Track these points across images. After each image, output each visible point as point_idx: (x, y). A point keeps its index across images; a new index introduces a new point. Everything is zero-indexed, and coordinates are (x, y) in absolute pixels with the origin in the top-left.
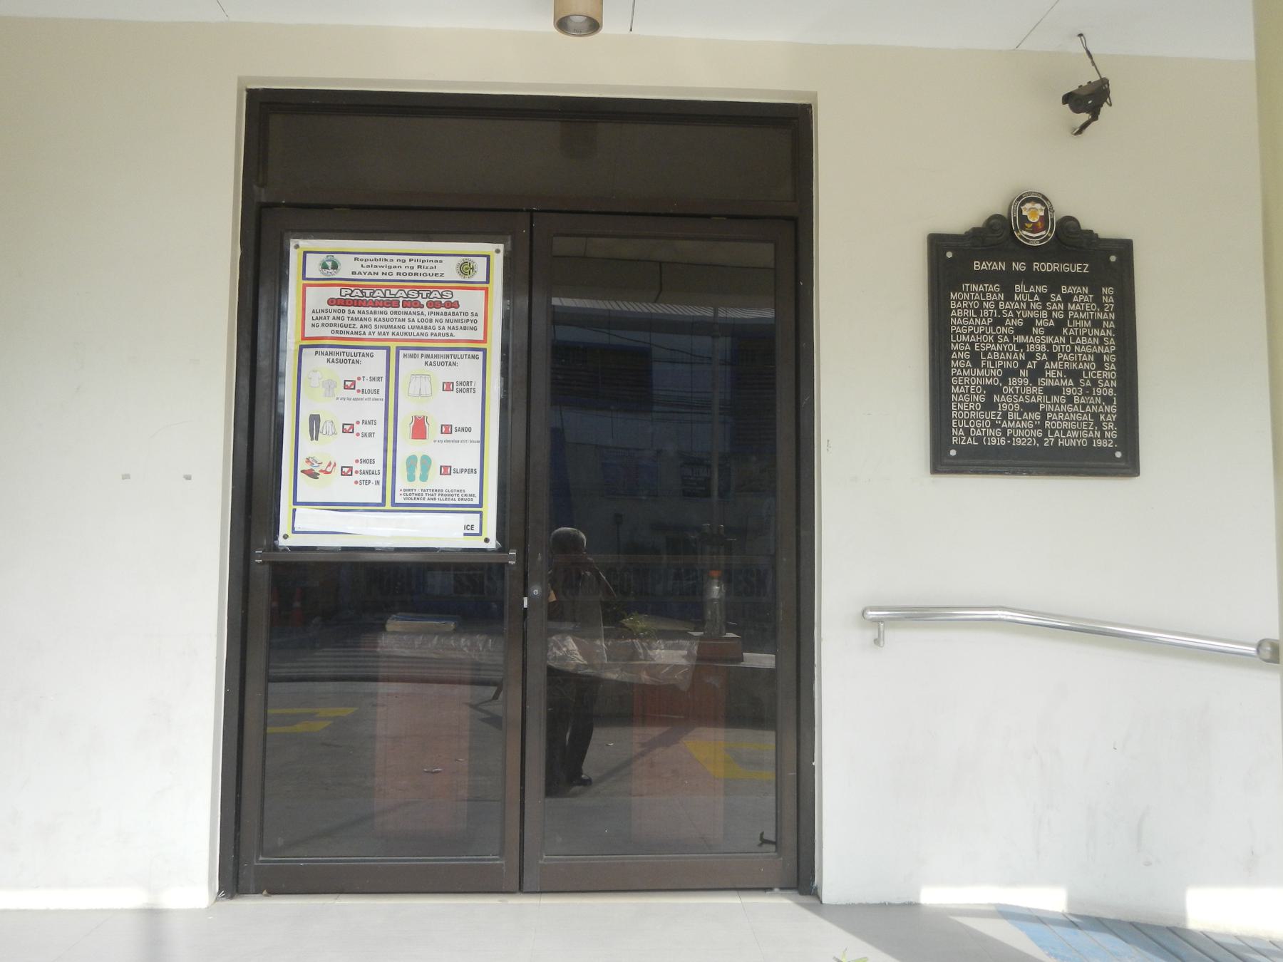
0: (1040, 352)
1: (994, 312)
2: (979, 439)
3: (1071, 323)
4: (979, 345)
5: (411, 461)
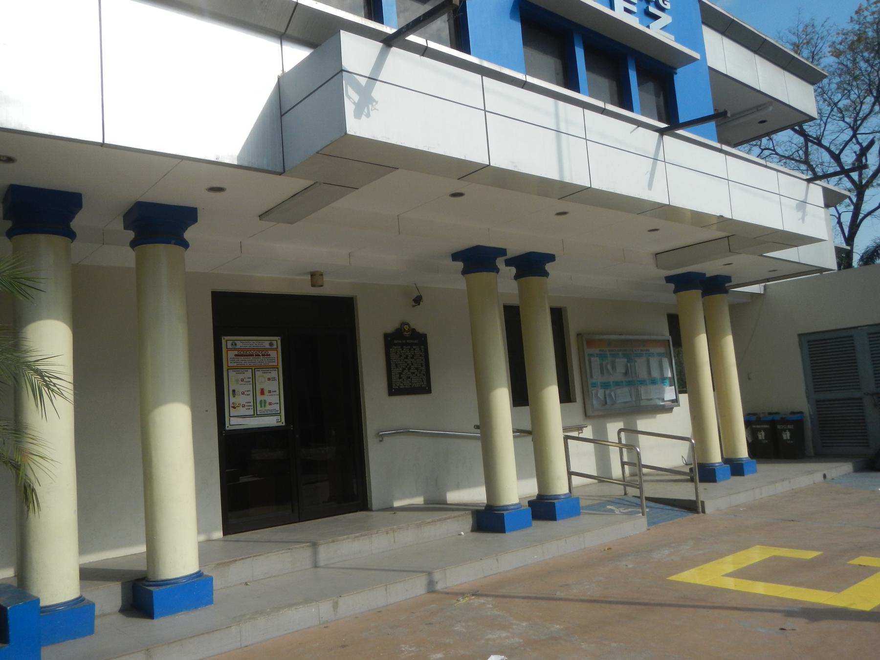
2: (398, 386)
5: (261, 402)
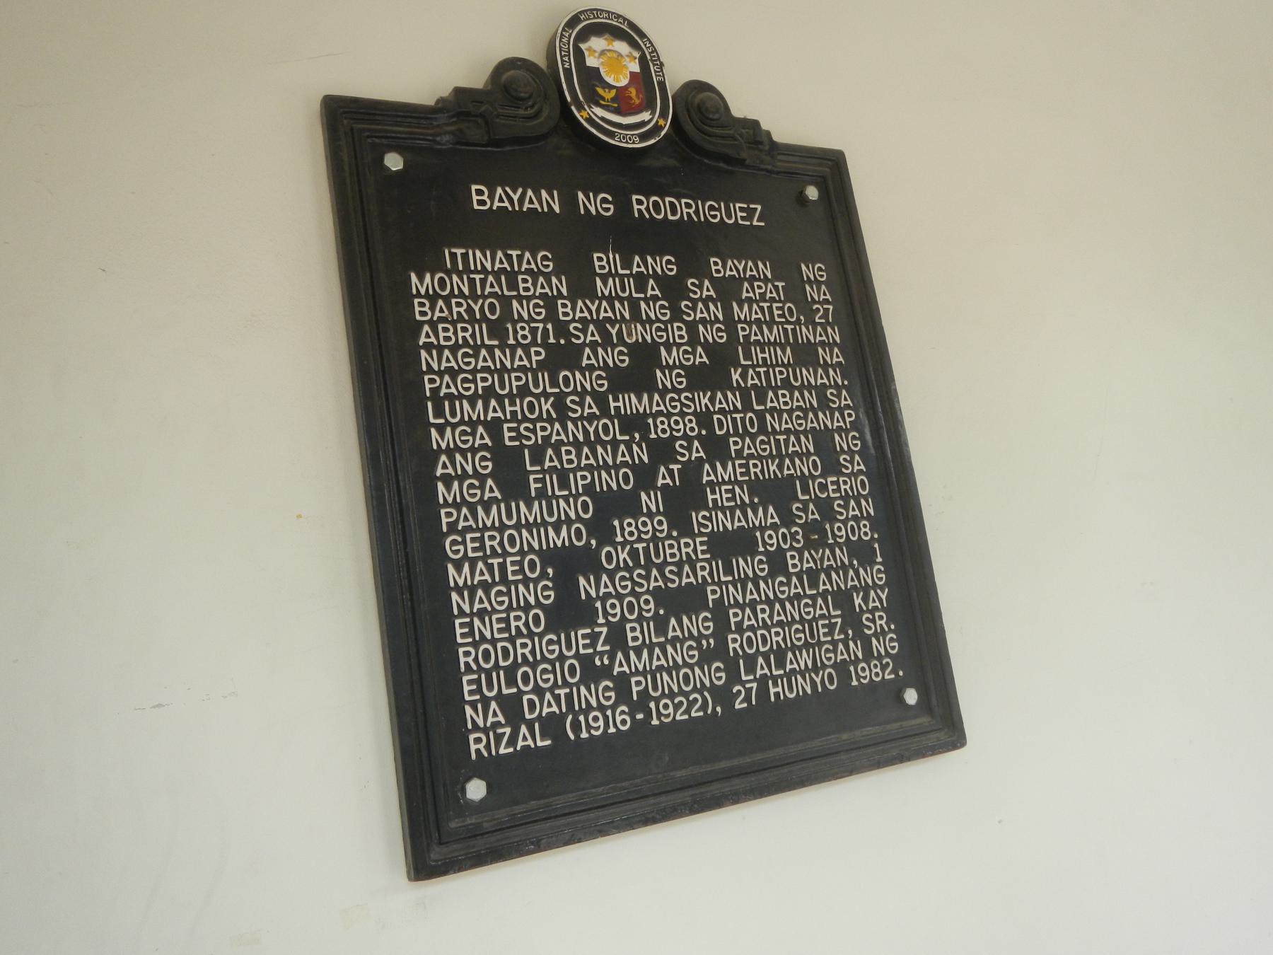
0: (685, 437)
1: (545, 330)
2: (552, 725)
3: (748, 356)
4: (516, 430)
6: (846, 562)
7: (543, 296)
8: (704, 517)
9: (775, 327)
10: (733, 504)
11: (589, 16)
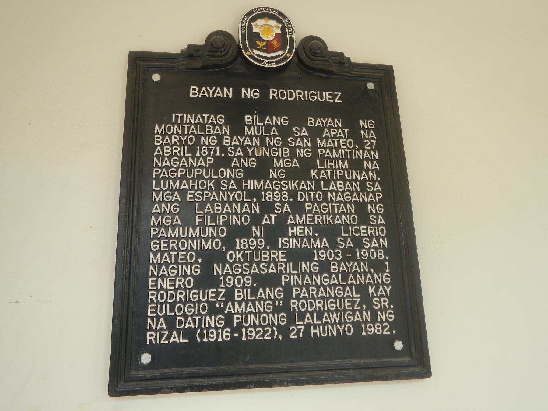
0: (281, 201)
1: (216, 150)
2: (189, 333)
3: (322, 164)
4: (194, 194)
6: (367, 270)
7: (217, 135)
8: (285, 241)
9: (340, 151)
10: (303, 235)
11: (258, 10)
